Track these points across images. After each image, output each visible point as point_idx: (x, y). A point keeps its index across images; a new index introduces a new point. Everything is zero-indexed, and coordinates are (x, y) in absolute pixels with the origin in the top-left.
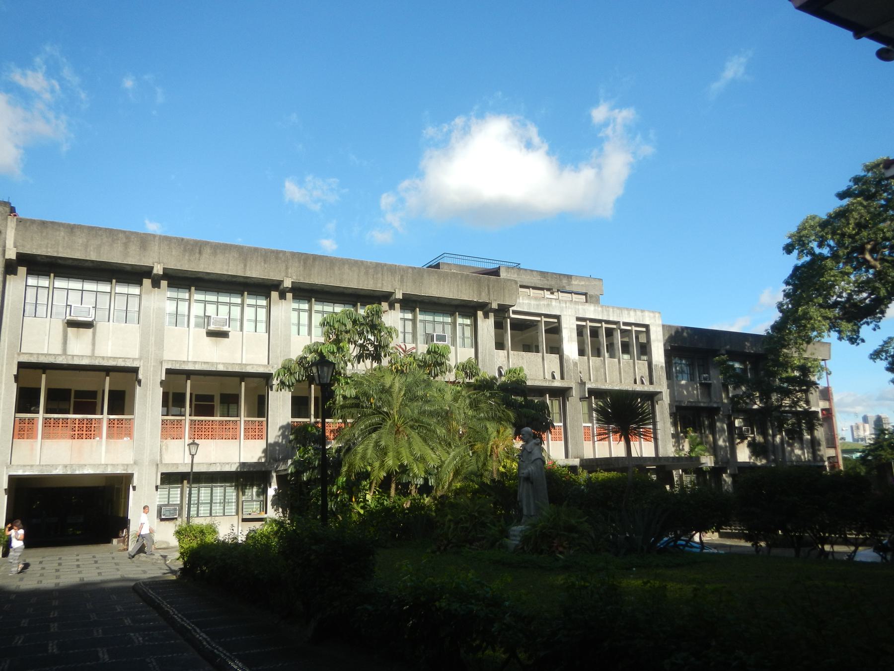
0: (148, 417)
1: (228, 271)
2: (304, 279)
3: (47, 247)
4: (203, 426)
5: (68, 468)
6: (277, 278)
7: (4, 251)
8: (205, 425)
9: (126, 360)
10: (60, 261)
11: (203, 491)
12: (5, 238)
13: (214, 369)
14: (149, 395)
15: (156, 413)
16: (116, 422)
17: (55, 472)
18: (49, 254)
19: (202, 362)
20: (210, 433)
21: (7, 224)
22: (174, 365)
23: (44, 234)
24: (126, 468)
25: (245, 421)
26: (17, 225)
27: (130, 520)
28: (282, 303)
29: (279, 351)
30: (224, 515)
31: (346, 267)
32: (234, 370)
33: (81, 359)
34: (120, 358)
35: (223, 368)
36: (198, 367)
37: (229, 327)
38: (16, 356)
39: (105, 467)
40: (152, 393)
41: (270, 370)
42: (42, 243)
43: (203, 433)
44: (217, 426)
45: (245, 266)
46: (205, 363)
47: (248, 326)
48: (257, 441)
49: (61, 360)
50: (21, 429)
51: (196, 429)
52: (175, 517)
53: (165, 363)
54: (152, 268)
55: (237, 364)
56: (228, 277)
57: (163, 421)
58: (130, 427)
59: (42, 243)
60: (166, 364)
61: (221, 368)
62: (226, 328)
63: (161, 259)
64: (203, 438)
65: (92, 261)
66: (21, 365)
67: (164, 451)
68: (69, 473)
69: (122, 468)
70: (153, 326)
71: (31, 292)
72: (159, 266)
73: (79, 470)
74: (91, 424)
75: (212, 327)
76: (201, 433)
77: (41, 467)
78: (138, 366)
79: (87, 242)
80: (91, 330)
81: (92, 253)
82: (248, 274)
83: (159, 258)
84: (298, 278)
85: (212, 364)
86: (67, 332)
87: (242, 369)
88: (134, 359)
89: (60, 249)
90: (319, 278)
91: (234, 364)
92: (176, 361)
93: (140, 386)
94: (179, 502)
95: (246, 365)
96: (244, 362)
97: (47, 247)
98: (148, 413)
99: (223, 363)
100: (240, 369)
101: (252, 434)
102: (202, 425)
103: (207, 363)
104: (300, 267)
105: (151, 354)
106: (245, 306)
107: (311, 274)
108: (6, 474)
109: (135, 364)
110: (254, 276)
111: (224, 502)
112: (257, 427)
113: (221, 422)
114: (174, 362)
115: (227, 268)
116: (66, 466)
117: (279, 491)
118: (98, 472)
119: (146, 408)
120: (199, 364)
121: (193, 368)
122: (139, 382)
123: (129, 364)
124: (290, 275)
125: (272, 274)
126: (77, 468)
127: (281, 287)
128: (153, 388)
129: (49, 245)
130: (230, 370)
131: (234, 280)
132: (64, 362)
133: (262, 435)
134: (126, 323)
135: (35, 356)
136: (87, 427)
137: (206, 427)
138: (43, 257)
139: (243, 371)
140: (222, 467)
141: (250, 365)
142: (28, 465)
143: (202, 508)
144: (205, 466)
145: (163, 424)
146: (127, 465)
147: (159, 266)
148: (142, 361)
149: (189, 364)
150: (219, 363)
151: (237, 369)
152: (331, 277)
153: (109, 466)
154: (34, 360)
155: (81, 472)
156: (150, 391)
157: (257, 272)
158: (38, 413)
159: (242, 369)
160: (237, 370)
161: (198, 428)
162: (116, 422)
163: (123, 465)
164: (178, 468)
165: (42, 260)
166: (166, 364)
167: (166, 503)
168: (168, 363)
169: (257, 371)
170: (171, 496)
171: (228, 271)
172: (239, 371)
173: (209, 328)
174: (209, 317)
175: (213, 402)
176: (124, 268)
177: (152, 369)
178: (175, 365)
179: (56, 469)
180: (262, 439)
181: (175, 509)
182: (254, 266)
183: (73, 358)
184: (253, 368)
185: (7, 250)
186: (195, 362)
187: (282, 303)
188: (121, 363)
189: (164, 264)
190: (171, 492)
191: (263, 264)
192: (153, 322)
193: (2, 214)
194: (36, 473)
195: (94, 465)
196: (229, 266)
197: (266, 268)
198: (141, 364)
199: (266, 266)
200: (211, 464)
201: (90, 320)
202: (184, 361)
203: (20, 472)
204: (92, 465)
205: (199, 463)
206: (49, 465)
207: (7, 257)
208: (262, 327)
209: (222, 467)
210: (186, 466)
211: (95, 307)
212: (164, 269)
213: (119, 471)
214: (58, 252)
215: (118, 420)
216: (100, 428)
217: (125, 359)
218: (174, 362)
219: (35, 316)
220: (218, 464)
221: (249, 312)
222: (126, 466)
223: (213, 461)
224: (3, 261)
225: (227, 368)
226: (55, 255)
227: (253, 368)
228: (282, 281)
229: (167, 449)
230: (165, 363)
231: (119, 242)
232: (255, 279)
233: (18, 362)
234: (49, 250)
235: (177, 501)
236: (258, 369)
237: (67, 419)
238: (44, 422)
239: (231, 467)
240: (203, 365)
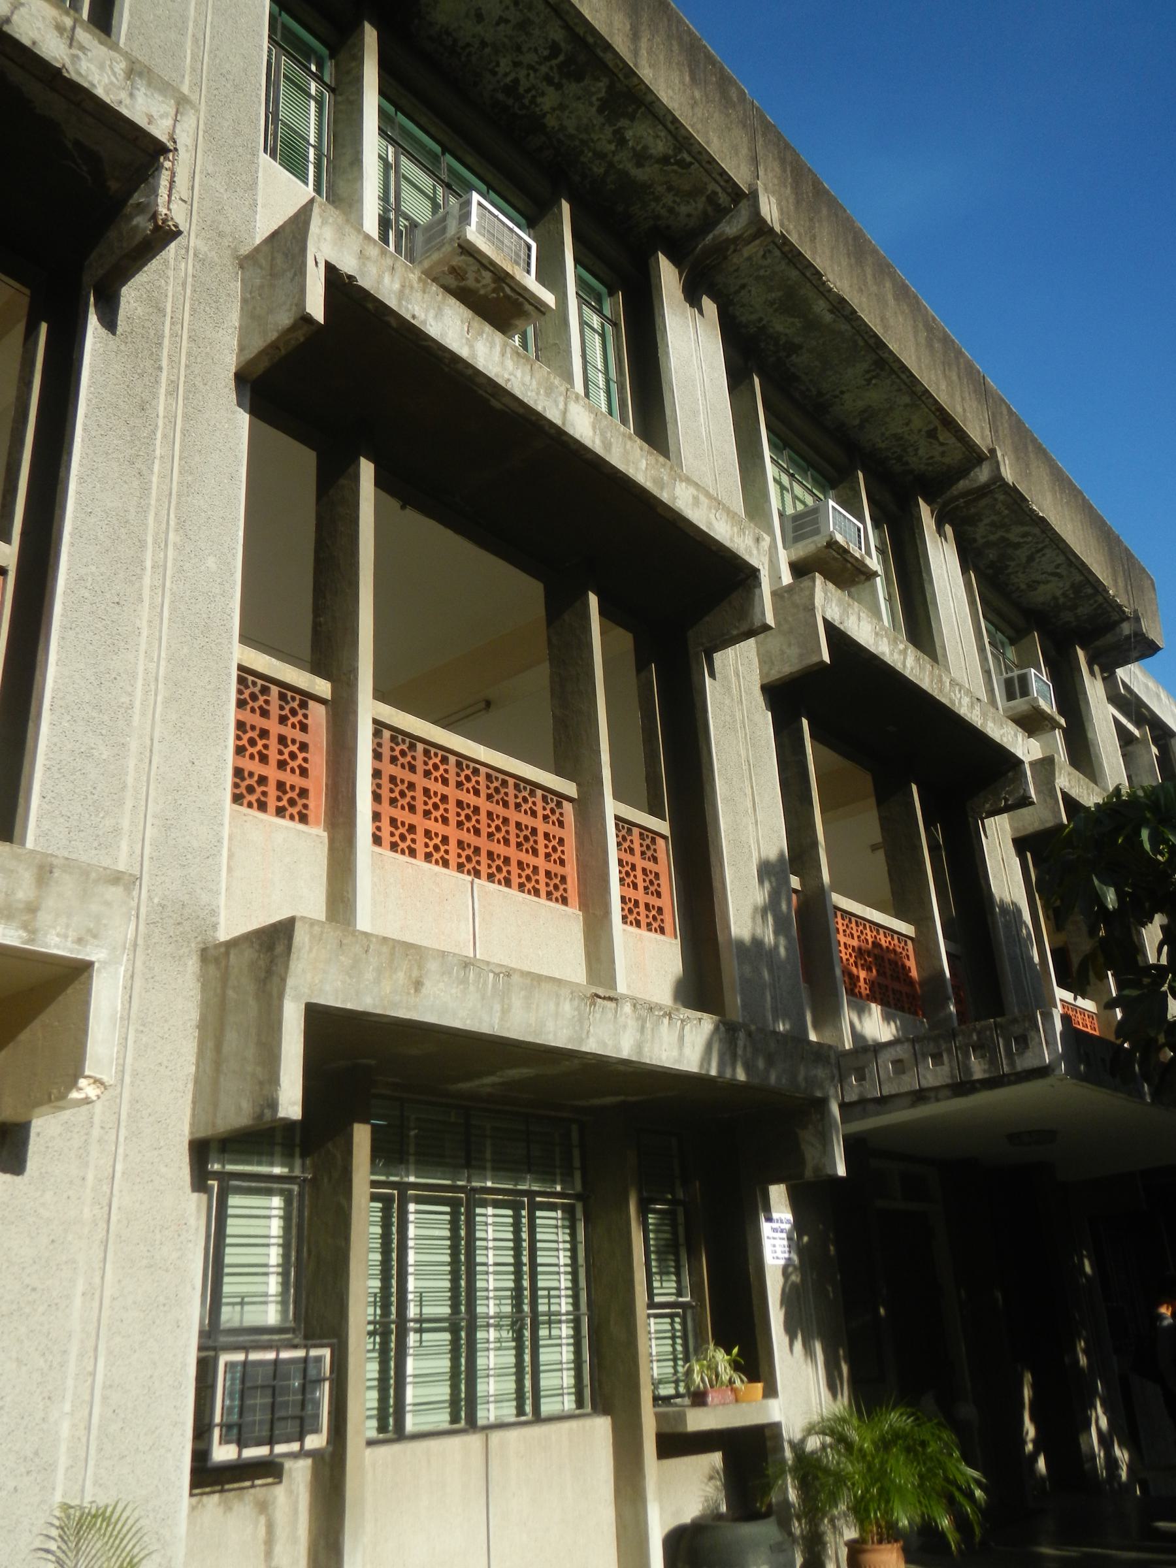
0: (160, 567)
15: (211, 562)
35: (591, 433)
40: (186, 417)
56: (555, 50)
87: (661, 485)
93: (110, 323)
117: (800, 1237)
119: (145, 490)
127: (730, 228)
128: (191, 390)
140: (642, 1029)
164: (418, 985)
169: (710, 524)
170: (231, 1256)
172: (649, 485)
182: (661, 57)
190: (233, 1227)
210: (464, 981)
220: (627, 1008)
225: (607, 446)
235: (262, 1299)
240: (509, 364)
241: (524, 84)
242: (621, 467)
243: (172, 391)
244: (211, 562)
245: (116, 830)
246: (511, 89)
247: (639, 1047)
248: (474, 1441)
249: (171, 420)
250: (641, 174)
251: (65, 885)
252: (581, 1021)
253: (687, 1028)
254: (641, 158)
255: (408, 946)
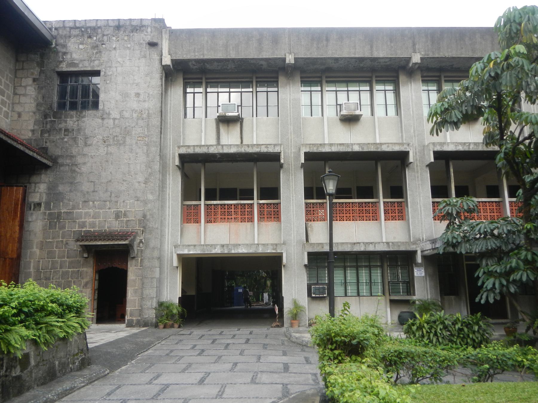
0: (293, 200)
1: (355, 54)
2: (433, 53)
3: (194, 51)
4: (344, 209)
5: (225, 247)
6: (405, 55)
7: (161, 60)
8: (346, 207)
9: (268, 146)
10: (208, 66)
11: (349, 272)
12: (162, 48)
13: (349, 150)
14: (292, 179)
15: (300, 196)
16: (265, 206)
17: (214, 251)
18: (197, 57)
19: (337, 144)
20: (351, 215)
21: (162, 37)
22: (312, 148)
23: (191, 41)
24: (275, 247)
25: (384, 202)
26: (169, 36)
27: (283, 298)
28: (411, 83)
29: (412, 131)
30: (371, 295)
31: (477, 36)
32: (370, 150)
33: (229, 148)
34: (262, 145)
35: (359, 148)
36: (334, 149)
37: (361, 111)
38: (177, 148)
39: (257, 247)
41: (406, 148)
42: (191, 48)
43: (345, 215)
44: (358, 208)
45: (372, 47)
46: (340, 144)
47: (379, 111)
48: (397, 222)
49: (212, 150)
50: (189, 214)
51: (338, 211)
52: (325, 295)
53: (303, 147)
54: (284, 60)
55: (372, 144)
57: (306, 204)
58: (278, 211)
59: (191, 48)
60: (304, 148)
61: (356, 149)
62: (358, 112)
63: (292, 50)
64: (345, 219)
65: (233, 60)
66: (182, 157)
67: (309, 232)
68: (226, 252)
69: (272, 247)
70: (290, 116)
71: (190, 97)
72: (290, 56)
73: (235, 250)
74: (245, 209)
75: (344, 112)
76: (343, 215)
77: (202, 247)
78: (279, 151)
79: (227, 42)
80: (239, 125)
81: (231, 52)
82: (376, 55)
83: (290, 50)
84: (427, 53)
85: (348, 145)
86: (220, 129)
87: (378, 148)
88: (275, 145)
89: (205, 52)
90: (449, 50)
91: (369, 144)
92: (313, 144)
94: (327, 282)
95: (381, 144)
96: (378, 142)
97: (194, 51)
98: (293, 197)
99: (359, 144)
100: (376, 149)
101: (393, 215)
102: (343, 207)
103: (343, 144)
104: (427, 42)
105: (291, 142)
106: (374, 91)
107: (440, 48)
108: (175, 253)
109: (277, 150)
110: (381, 56)
111: (370, 283)
112: (396, 208)
113: (360, 204)
114: (311, 146)
115: (354, 50)
116: (223, 246)
118: (251, 251)
119: (290, 191)
120: (335, 146)
121: (330, 151)
122: (281, 166)
123: (271, 150)
124: (417, 51)
125: (399, 52)
126: (233, 247)
127: (411, 65)
128: (295, 173)
129: (196, 50)
130: (366, 149)
131: (362, 65)
132: (216, 152)
133: (402, 216)
134: (268, 116)
135: (192, 148)
136: (241, 211)
137: (347, 209)
138: (194, 63)
139: (379, 150)
140: (366, 246)
141: (385, 144)
142: (192, 245)
143: (349, 288)
144: (349, 246)
145: (307, 208)
146: (276, 245)
147: (290, 56)
148: (282, 146)
149: (326, 146)
150: (354, 144)
151: (372, 149)
152: (462, 48)
153: (260, 246)
154: (191, 151)
155: (236, 252)
156: (292, 175)
157: (384, 52)
158: (200, 200)
159: (378, 148)
160: (372, 150)
161: (339, 210)
162: (265, 206)
163: (272, 244)
164: (323, 247)
165: (195, 67)
166: (304, 148)
167: (315, 282)
168: (306, 147)
169: (392, 149)
171: (355, 54)
172: (375, 150)
173: (342, 113)
174: (340, 105)
175: (351, 194)
176: (262, 65)
177: (292, 155)
178: (313, 149)
179: (215, 248)
180: (403, 220)
181: (324, 288)
183: (223, 147)
184: (388, 146)
185: (163, 58)
186: (331, 145)
187: (411, 83)
188: (264, 150)
189: (295, 54)
191: (389, 43)
192: (290, 113)
193: (158, 29)
194: (199, 252)
195: (247, 245)
196: (355, 49)
197: (392, 47)
198: (282, 149)
199: (392, 45)
200: (355, 243)
201: (236, 114)
202: (321, 144)
203: (186, 252)
204: (245, 244)
205: (343, 243)
206: (208, 245)
207: (164, 63)
208: (392, 110)
209: (366, 246)
211: (241, 106)
212: (295, 59)
213: (270, 250)
214: (203, 55)
215: (267, 204)
216: (252, 213)
217: (267, 145)
218: (311, 146)
219: (194, 118)
220: (362, 244)
221: (379, 97)
222: (275, 246)
223: (355, 242)
224: (161, 68)
225: (363, 148)
226: (202, 57)
227: (388, 146)
228: (410, 58)
229: (312, 231)
230: (303, 147)
231: (254, 39)
232: (383, 60)
233: (179, 154)
234: (196, 54)
236: (393, 147)
237: (225, 205)
238: (206, 208)
239: (375, 246)
240: (339, 147)
241: (356, 66)
242: (367, 150)
243: (292, 175)
244: (300, 196)
245: (291, 234)
246: (354, 67)
247: (365, 249)
248: (357, 298)
249: (292, 179)
250: (388, 63)
251: (279, 246)
252: (352, 247)
253: (376, 245)
254: (386, 62)
255: (320, 243)
